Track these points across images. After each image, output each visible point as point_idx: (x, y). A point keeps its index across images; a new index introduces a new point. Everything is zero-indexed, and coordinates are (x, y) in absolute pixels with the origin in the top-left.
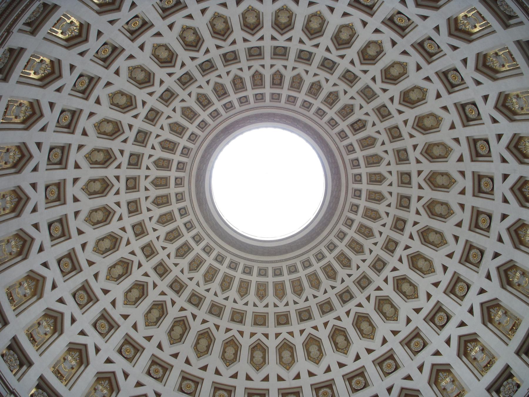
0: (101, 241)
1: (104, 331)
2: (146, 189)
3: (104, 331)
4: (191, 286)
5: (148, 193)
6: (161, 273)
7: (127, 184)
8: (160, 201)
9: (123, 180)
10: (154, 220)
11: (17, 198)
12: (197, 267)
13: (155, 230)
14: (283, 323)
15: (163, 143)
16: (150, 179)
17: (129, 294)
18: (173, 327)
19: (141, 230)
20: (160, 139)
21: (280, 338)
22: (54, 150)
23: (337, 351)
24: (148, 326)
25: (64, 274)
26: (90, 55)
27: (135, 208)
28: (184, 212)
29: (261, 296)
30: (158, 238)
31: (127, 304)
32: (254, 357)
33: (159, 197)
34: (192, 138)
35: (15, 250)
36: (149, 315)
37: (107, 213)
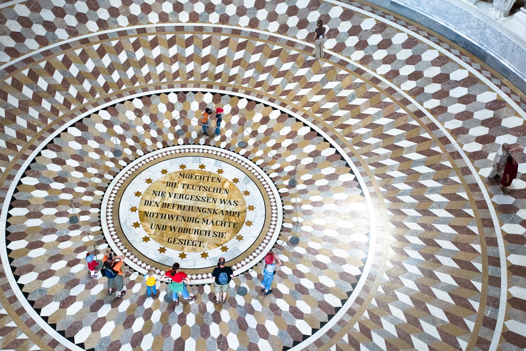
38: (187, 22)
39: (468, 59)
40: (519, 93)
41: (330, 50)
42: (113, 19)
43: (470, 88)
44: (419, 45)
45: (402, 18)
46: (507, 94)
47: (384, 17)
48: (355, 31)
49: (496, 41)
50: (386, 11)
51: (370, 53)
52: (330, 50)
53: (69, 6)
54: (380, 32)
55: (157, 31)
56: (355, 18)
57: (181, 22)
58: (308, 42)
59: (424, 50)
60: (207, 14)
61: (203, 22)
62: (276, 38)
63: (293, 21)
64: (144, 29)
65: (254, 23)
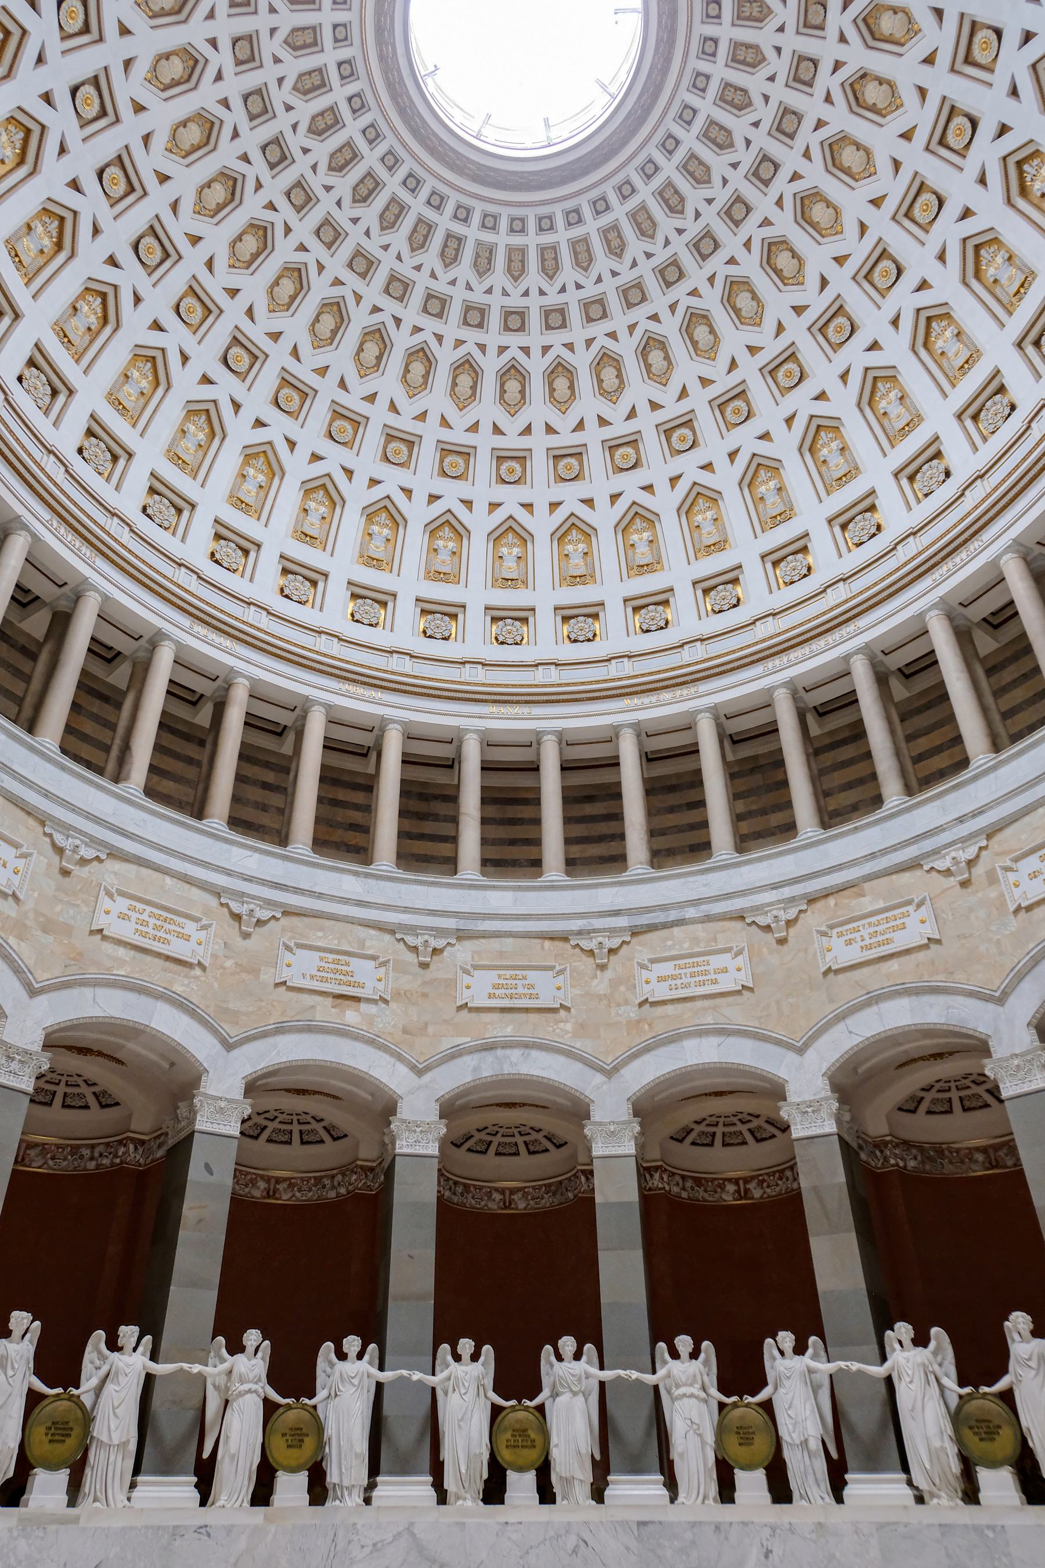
0: (317, 325)
1: (403, 457)
2: (328, 189)
3: (403, 457)
4: (496, 303)
5: (335, 195)
6: (438, 310)
7: (292, 203)
8: (363, 191)
9: (281, 202)
10: (375, 230)
11: (147, 361)
12: (490, 263)
13: (386, 248)
14: (675, 279)
15: (299, 85)
16: (323, 167)
17: (409, 376)
18: (502, 385)
19: (364, 262)
20: (288, 84)
21: (680, 310)
22: (140, 246)
23: (785, 284)
24: (465, 407)
25: (296, 414)
26: (54, 46)
27: (332, 233)
28: (414, 182)
29: (618, 251)
30: (399, 257)
31: (415, 395)
32: (650, 365)
33: (357, 185)
34: (340, 37)
35: (201, 436)
36: (457, 389)
37: (296, 274)
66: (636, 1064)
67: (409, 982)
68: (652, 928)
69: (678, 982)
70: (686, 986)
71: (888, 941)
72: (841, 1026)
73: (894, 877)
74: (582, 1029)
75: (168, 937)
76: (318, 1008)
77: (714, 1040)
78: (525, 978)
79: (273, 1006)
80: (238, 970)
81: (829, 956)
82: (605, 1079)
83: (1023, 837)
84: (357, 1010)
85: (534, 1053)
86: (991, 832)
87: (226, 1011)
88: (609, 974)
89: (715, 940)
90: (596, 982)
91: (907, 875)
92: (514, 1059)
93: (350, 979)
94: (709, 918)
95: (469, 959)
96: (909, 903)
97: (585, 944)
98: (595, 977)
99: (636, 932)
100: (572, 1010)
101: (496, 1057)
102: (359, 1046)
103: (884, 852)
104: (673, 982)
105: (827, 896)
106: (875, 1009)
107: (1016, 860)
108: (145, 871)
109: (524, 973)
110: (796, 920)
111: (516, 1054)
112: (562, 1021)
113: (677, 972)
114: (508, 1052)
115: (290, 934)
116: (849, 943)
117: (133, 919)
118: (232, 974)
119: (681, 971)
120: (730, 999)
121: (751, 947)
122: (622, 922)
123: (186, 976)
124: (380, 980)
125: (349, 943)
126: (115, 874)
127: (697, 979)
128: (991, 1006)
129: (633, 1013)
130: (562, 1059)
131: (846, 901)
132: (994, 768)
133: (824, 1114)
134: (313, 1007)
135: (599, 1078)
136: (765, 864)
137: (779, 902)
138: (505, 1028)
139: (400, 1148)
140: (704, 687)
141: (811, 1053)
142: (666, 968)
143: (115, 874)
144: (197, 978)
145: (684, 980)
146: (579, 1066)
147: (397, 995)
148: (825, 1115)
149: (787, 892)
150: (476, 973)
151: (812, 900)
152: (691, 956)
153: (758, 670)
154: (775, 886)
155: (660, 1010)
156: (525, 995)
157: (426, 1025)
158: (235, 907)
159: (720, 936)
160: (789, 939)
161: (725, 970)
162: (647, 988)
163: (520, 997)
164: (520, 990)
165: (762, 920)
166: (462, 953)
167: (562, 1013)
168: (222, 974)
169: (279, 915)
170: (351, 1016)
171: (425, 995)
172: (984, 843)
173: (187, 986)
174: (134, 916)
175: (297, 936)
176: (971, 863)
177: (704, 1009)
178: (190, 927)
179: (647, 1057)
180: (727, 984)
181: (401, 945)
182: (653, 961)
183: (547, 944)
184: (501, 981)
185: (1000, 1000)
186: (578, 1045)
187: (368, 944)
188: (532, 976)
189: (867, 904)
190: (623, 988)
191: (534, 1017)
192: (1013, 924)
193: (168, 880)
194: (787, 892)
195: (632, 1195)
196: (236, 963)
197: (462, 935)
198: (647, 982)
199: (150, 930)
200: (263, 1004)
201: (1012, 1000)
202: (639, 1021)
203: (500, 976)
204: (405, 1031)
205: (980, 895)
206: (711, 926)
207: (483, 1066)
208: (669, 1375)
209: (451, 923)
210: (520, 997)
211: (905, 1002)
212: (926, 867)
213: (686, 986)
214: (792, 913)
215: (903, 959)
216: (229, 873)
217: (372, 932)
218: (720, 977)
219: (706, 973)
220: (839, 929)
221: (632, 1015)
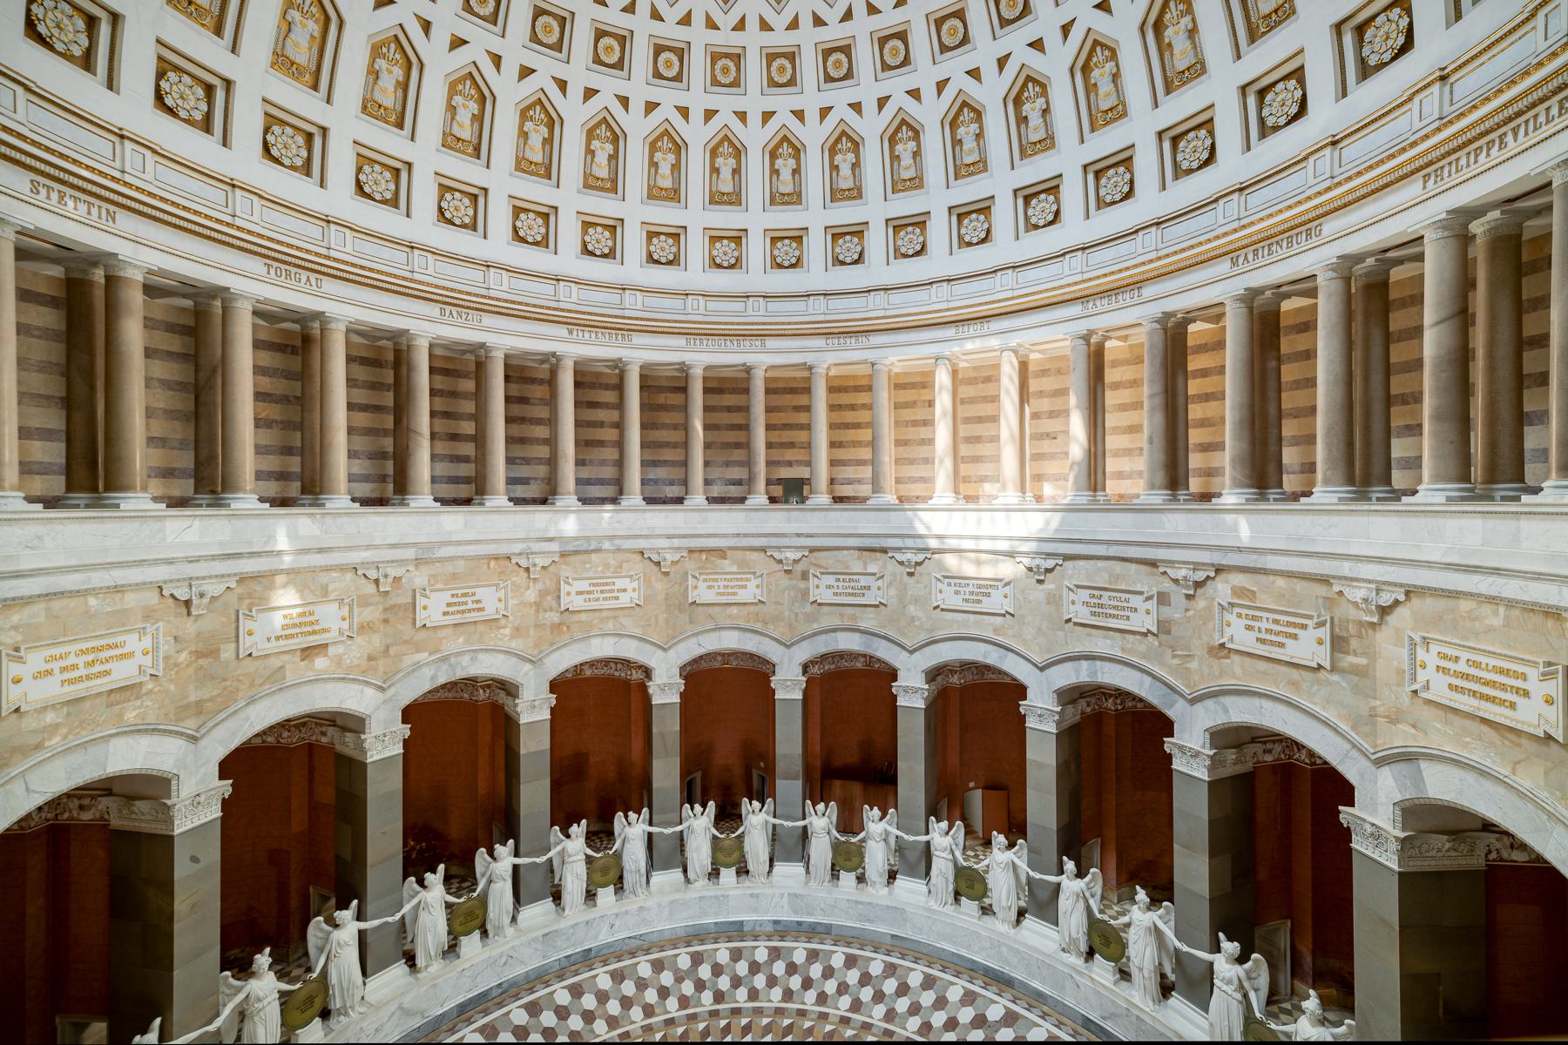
38: (678, 1010)
39: (995, 989)
40: (1068, 1022)
41: (847, 1011)
42: (589, 1027)
43: (1015, 1027)
44: (938, 982)
45: (908, 952)
46: (1055, 1026)
47: (888, 955)
48: (865, 979)
49: (1016, 960)
50: (889, 948)
51: (891, 1005)
52: (847, 1011)
53: (533, 1021)
54: (893, 975)
55: (643, 1032)
56: (860, 962)
57: (669, 1012)
58: (819, 1005)
59: (946, 989)
60: (698, 994)
61: (695, 1006)
62: (783, 1009)
63: (795, 982)
64: (628, 1032)
65: (753, 995)
66: (555, 656)
67: (372, 614)
68: (576, 552)
69: (591, 596)
70: (598, 599)
71: (735, 594)
72: (694, 640)
73: (747, 553)
74: (517, 631)
75: (106, 667)
76: (288, 666)
77: (612, 640)
78: (474, 594)
79: (240, 681)
80: (193, 658)
81: (696, 593)
82: (531, 666)
83: (831, 562)
84: (326, 655)
85: (481, 656)
86: (813, 550)
87: (187, 706)
88: (540, 586)
89: (621, 567)
90: (528, 592)
91: (756, 554)
92: (464, 664)
93: (316, 628)
94: (619, 550)
95: (426, 582)
96: (754, 573)
97: (524, 563)
98: (528, 588)
99: (563, 555)
100: (511, 618)
101: (450, 665)
102: (330, 686)
103: (746, 535)
104: (587, 596)
105: (701, 551)
106: (717, 633)
107: (822, 573)
108: (57, 605)
109: (473, 590)
110: (678, 561)
111: (466, 659)
112: (503, 627)
113: (592, 588)
114: (459, 659)
115: (247, 601)
116: (710, 587)
117: (57, 671)
118: (187, 666)
119: (595, 589)
120: (626, 612)
121: (645, 575)
122: (555, 547)
123: (137, 698)
124: (344, 619)
125: (312, 592)
126: (15, 628)
127: (605, 595)
128: (782, 648)
129: (554, 617)
130: (502, 657)
131: (713, 559)
132: (827, 510)
133: (674, 691)
134: (282, 667)
135: (528, 666)
136: (663, 514)
137: (670, 548)
138: (455, 643)
139: (371, 757)
140: (638, 339)
141: (672, 653)
142: (584, 585)
143: (15, 628)
144: (150, 692)
145: (596, 596)
146: (514, 660)
147: (365, 628)
148: (674, 691)
149: (676, 543)
150: (433, 595)
151: (691, 551)
152: (603, 578)
153: (680, 341)
154: (670, 537)
155: (576, 617)
156: (474, 610)
157: (388, 647)
158: (182, 594)
159: (624, 565)
160: (672, 574)
161: (625, 590)
162: (568, 599)
163: (469, 611)
164: (470, 606)
165: (655, 558)
166: (419, 578)
167: (503, 622)
168: (177, 673)
169: (233, 585)
170: (320, 663)
171: (386, 621)
172: (807, 554)
173: (140, 708)
174: (56, 666)
175: (256, 601)
176: (796, 562)
177: (608, 618)
178: (133, 642)
179: (564, 651)
180: (625, 600)
181: (363, 580)
182: (574, 579)
183: (493, 563)
184: (455, 600)
185: (788, 647)
186: (513, 644)
187: (330, 589)
188: (481, 593)
189: (727, 565)
190: (549, 598)
191: (481, 628)
192: (809, 608)
193: (92, 601)
194: (676, 543)
195: (546, 744)
196: (191, 653)
197: (418, 562)
198: (569, 594)
199: (82, 672)
200: (228, 683)
201: (794, 648)
202: (560, 624)
203: (453, 596)
204: (370, 658)
205: (794, 582)
206: (620, 556)
207: (439, 673)
208: (562, 853)
209: (410, 554)
210: (469, 611)
211: (736, 634)
212: (768, 554)
213: (598, 599)
214: (677, 557)
215: (740, 608)
216: (169, 562)
217: (334, 574)
218: (621, 595)
219: (611, 591)
220: (705, 577)
221: (555, 619)
